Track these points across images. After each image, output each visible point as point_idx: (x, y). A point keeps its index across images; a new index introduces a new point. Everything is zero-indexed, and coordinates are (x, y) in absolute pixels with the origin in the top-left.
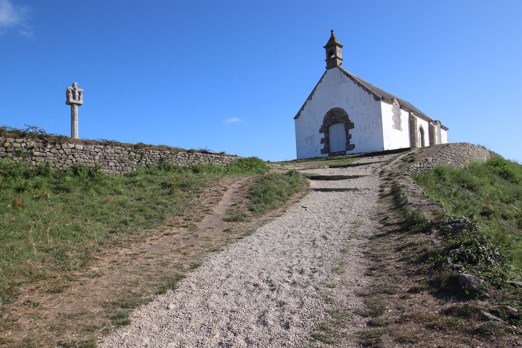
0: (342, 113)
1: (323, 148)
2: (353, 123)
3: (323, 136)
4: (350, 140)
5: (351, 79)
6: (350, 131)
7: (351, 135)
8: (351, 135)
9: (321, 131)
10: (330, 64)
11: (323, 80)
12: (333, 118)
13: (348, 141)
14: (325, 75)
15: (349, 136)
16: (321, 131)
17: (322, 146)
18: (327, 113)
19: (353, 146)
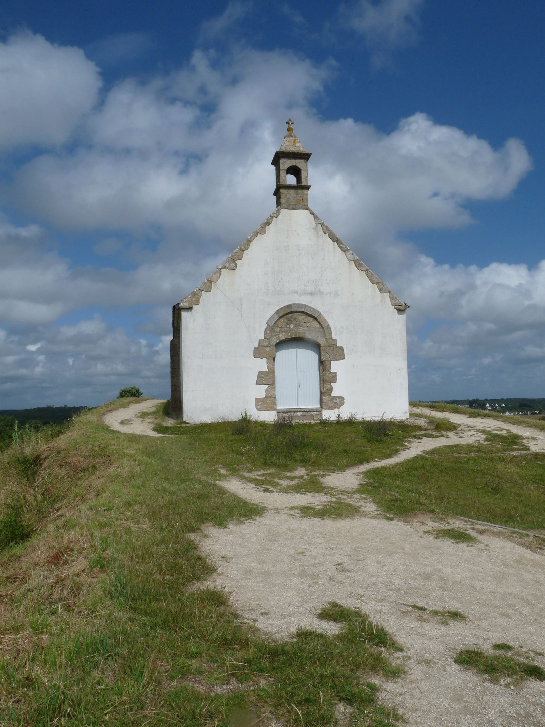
0: (315, 319)
1: (263, 395)
2: (342, 348)
3: (262, 365)
4: (332, 384)
5: (340, 247)
6: (335, 366)
7: (336, 373)
8: (336, 373)
9: (258, 353)
10: (290, 197)
11: (270, 229)
12: (292, 326)
13: (328, 386)
14: (274, 219)
15: (331, 375)
16: (258, 353)
17: (261, 391)
18: (277, 312)
19: (339, 402)
